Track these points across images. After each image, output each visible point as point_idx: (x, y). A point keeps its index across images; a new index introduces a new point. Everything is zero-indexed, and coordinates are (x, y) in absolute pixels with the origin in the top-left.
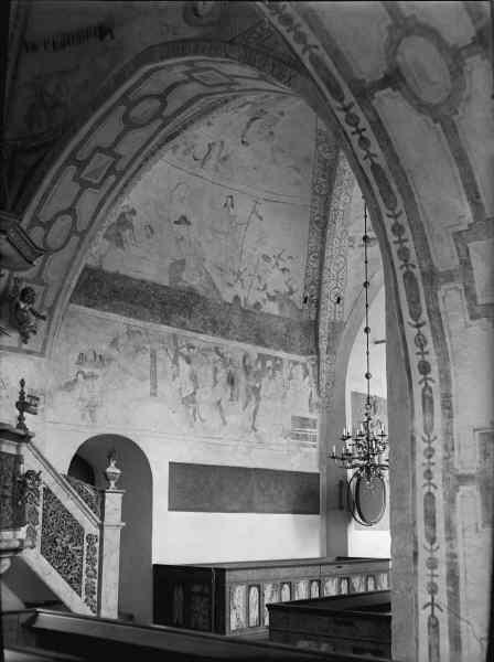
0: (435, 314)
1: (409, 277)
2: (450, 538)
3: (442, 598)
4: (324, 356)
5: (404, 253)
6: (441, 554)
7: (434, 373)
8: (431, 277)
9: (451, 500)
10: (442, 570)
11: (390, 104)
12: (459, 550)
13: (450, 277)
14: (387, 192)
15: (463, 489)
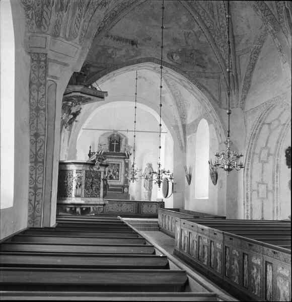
0: (253, 160)
1: (250, 153)
2: (251, 200)
3: (249, 212)
4: (72, 132)
5: (251, 148)
6: (249, 204)
7: (249, 170)
8: (254, 153)
9: (251, 194)
10: (249, 207)
11: (266, 127)
12: (253, 203)
13: (257, 154)
14: (253, 139)
15: (254, 192)
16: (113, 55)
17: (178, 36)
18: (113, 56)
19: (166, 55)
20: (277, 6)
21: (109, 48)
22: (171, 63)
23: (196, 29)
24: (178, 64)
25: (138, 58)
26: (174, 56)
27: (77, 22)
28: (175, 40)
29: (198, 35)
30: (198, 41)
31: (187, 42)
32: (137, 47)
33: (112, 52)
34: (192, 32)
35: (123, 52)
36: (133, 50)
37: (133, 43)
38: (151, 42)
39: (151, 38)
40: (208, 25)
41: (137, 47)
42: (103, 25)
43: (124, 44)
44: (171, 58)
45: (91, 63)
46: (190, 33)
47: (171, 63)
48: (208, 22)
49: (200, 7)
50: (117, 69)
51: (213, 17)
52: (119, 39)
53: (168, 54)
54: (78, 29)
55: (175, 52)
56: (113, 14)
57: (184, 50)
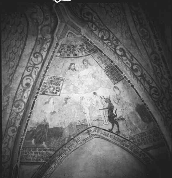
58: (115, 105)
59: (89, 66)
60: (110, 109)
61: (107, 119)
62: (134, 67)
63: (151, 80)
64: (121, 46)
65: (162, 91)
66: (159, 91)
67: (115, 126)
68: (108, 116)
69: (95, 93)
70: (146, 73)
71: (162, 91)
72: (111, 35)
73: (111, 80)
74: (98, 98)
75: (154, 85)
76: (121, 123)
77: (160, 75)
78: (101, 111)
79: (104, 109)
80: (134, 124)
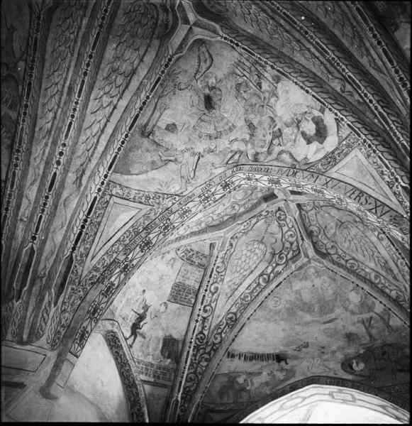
16: (248, 385)
17: (352, 329)
18: (248, 388)
19: (340, 365)
20: (395, 193)
21: (238, 374)
22: (350, 377)
23: (379, 308)
24: (364, 376)
25: (292, 381)
26: (354, 365)
27: (45, 315)
28: (350, 337)
29: (386, 317)
30: (388, 326)
31: (371, 336)
32: (287, 364)
33: (245, 381)
34: (374, 315)
35: (264, 377)
36: (282, 369)
37: (280, 358)
38: (309, 349)
39: (308, 343)
40: (393, 294)
41: (287, 364)
42: (219, 339)
43: (265, 363)
44: (349, 369)
45: (212, 406)
46: (371, 318)
47: (350, 377)
48: (391, 291)
49: (367, 270)
50: (257, 408)
51: (395, 278)
52: (254, 357)
53: (343, 364)
54: (46, 324)
55: (355, 358)
56: (232, 318)
57: (369, 350)
58: (148, 318)
59: (170, 267)
60: (141, 318)
61: (131, 324)
62: (208, 308)
63: (208, 327)
64: (219, 287)
65: (207, 342)
66: (205, 341)
67: (133, 337)
68: (134, 321)
69: (144, 291)
70: (210, 320)
71: (207, 342)
72: (224, 273)
73: (171, 295)
74: (140, 297)
75: (206, 333)
76: (139, 338)
77: (219, 331)
78: (132, 313)
79: (136, 313)
80: (150, 349)
